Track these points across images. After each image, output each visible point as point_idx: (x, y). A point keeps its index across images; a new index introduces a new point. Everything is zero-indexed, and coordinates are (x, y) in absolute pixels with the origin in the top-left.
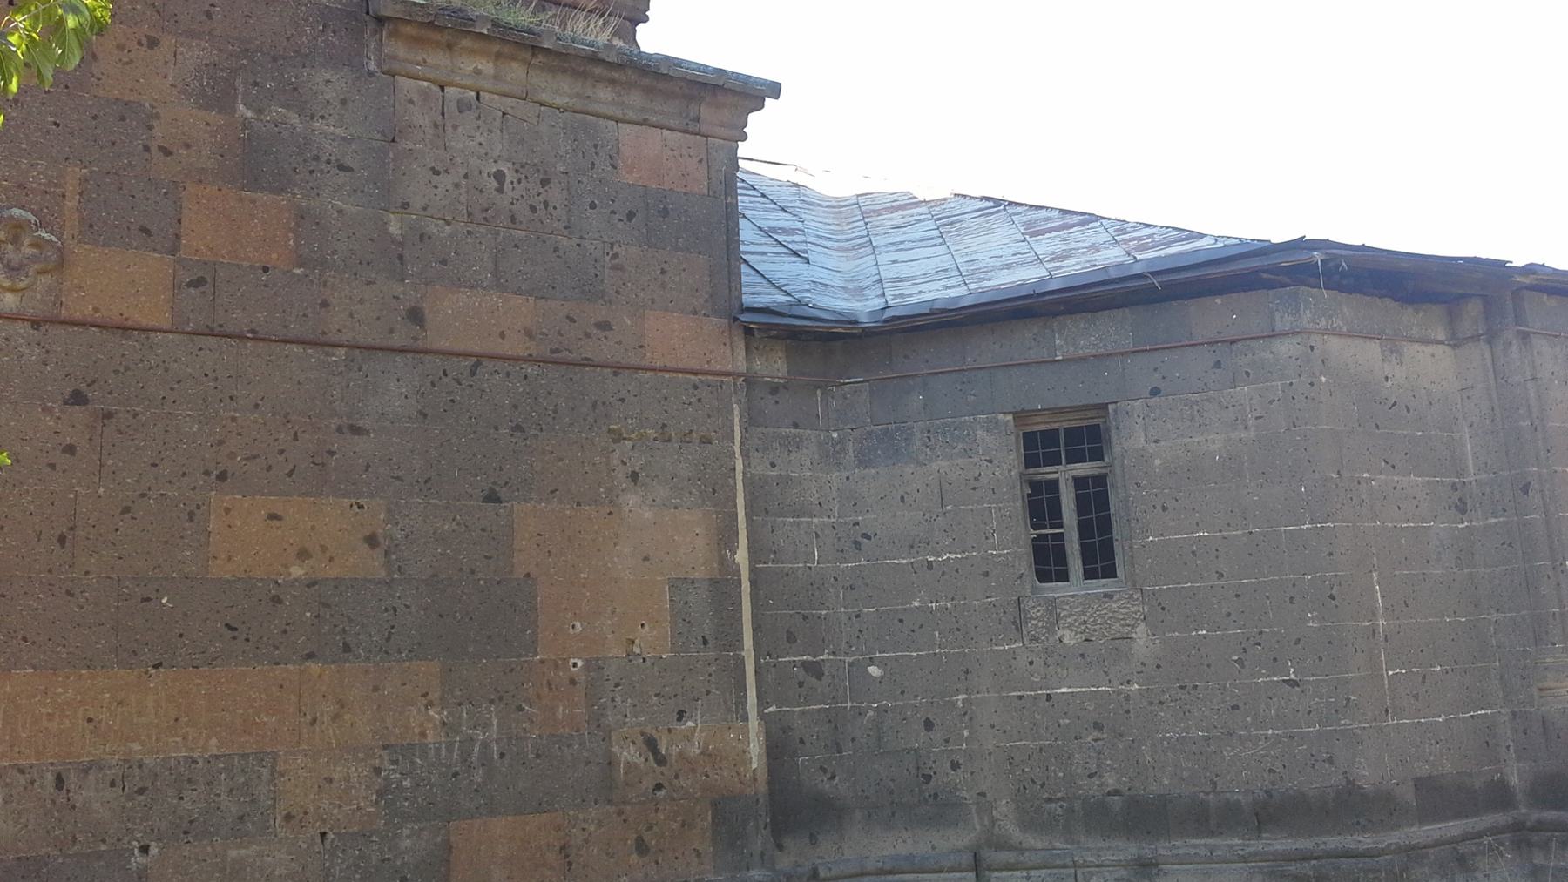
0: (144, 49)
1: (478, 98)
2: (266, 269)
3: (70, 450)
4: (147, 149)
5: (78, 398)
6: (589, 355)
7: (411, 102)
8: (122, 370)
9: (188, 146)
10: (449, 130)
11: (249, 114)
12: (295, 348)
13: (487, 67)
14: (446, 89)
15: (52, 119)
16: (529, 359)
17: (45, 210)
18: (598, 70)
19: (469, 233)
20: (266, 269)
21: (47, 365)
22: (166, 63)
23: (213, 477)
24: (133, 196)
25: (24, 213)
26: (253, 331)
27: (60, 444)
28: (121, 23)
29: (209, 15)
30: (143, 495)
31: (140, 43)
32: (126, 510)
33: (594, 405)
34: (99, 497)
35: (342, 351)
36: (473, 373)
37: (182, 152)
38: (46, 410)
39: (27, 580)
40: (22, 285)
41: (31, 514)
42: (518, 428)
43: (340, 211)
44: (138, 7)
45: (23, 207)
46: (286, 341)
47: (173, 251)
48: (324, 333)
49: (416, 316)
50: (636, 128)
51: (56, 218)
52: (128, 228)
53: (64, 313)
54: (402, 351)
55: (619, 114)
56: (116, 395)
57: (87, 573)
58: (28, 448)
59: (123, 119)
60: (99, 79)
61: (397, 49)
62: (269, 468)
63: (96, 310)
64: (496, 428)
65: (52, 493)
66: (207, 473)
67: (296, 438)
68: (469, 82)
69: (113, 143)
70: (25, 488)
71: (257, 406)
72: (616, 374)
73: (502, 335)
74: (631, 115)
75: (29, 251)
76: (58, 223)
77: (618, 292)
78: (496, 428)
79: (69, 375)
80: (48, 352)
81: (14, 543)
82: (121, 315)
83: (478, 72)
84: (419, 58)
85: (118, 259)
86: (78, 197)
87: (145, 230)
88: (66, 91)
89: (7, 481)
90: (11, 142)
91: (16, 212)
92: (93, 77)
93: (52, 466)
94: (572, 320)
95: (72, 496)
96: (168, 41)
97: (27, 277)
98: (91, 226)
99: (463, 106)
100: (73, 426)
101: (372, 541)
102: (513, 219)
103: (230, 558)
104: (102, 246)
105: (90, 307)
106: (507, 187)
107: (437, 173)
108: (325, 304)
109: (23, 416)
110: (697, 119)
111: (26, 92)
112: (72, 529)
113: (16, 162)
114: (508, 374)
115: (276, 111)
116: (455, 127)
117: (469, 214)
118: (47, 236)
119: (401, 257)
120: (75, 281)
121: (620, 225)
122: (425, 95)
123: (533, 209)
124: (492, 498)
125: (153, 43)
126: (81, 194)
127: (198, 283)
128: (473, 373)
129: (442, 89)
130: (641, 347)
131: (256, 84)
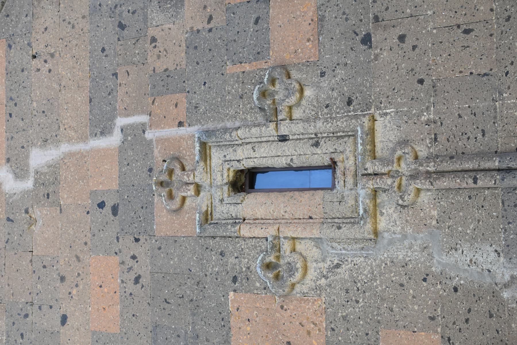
0: (157, 44)
3: (402, 38)
4: (210, 30)
5: (367, 40)
8: (345, 16)
9: (205, 7)
15: (203, 86)
17: (253, 81)
21: (347, 63)
22: (163, 30)
24: (238, 32)
25: (255, 92)
27: (399, 45)
28: (146, 59)
31: (155, 47)
34: (434, 13)
38: (377, 57)
39: (499, 50)
40: (297, 86)
41: (450, 55)
44: (137, 52)
51: (257, 74)
52: (257, 31)
56: (362, 17)
57: (492, 10)
58: (403, 65)
59: (196, 48)
60: (177, 65)
63: (309, 40)
65: (434, 44)
69: (210, 50)
70: (431, 62)
75: (277, 86)
76: (259, 73)
79: (352, 48)
80: (338, 64)
81: (472, 63)
82: (310, 24)
85: (276, 33)
86: (243, 64)
88: (186, 82)
89: (427, 74)
90: (218, 107)
91: (255, 97)
92: (176, 69)
93: (414, 47)
95: (435, 31)
96: (151, 32)
97: (291, 84)
98: (258, 53)
100: (386, 39)
104: (269, 44)
105: (308, 44)
109: (382, 72)
111: (190, 103)
113: (229, 102)
118: (267, 77)
120: (292, 56)
125: (154, 40)
126: (241, 63)
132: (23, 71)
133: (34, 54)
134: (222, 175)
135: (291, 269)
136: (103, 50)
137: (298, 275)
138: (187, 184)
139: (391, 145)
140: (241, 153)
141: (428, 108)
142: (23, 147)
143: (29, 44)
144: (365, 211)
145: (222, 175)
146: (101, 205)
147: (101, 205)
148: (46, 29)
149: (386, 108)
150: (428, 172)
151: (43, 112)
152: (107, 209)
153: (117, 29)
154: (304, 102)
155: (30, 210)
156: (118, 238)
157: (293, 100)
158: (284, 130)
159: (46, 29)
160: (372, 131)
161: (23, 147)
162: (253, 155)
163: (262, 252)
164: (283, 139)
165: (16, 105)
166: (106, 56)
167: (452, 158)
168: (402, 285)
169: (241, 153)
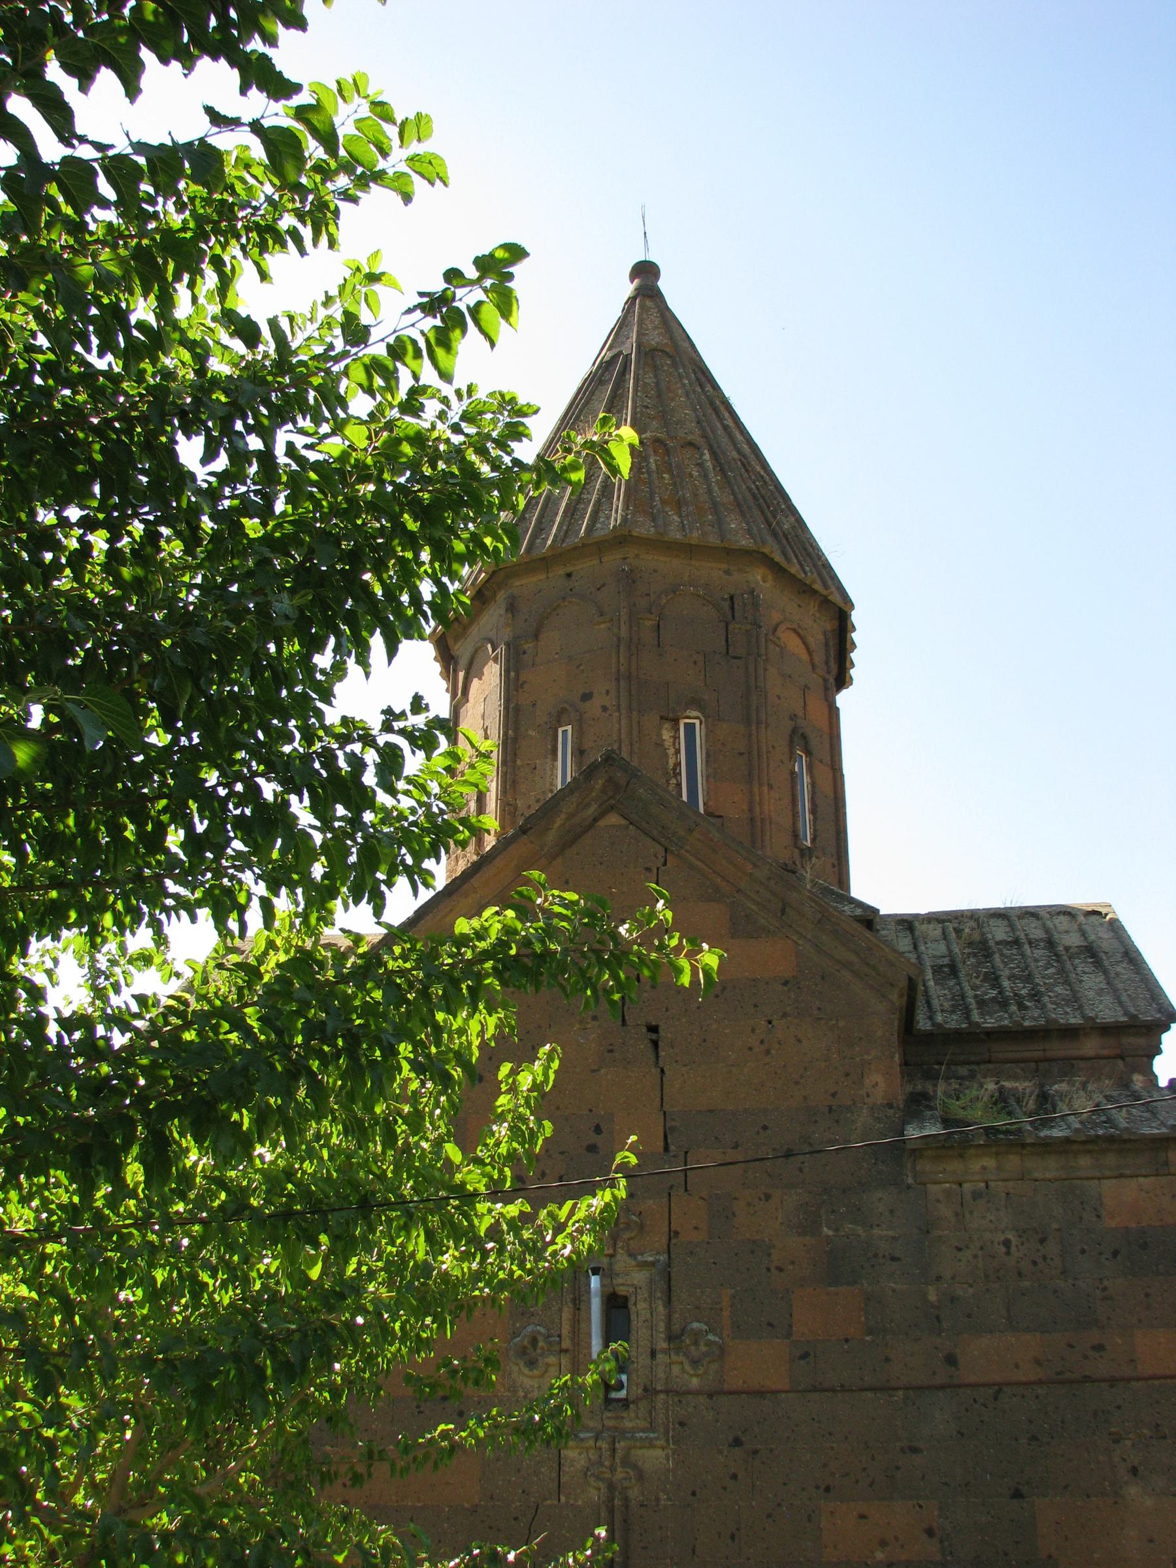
1: (987, 1187)
2: (847, 1340)
3: (734, 1477)
4: (769, 1270)
5: (737, 1442)
6: (1087, 1373)
7: (938, 1201)
9: (793, 1263)
10: (967, 1215)
11: (831, 1233)
12: (870, 1394)
13: (990, 1162)
14: (966, 1186)
16: (1040, 1382)
18: (1075, 1147)
19: (988, 1290)
20: (847, 1340)
23: (821, 1490)
26: (842, 1386)
29: (801, 1170)
30: (779, 1505)
31: (760, 1199)
32: (769, 1516)
33: (1095, 1414)
35: (901, 1393)
36: (996, 1398)
37: (791, 1267)
38: (720, 1452)
40: (700, 1372)
42: (1034, 1438)
43: (894, 1291)
45: (699, 1321)
46: (862, 1390)
47: (789, 1335)
48: (888, 1381)
49: (951, 1360)
50: (1114, 1181)
53: (726, 1387)
54: (942, 1387)
55: (1098, 1174)
59: (753, 1252)
61: (924, 1166)
62: (857, 1482)
63: (744, 1382)
64: (1016, 1439)
66: (817, 1487)
67: (873, 1459)
68: (977, 1178)
71: (846, 1438)
72: (1112, 1386)
73: (1017, 1366)
74: (1107, 1173)
75: (703, 1348)
77: (1109, 1318)
78: (1016, 1439)
83: (984, 1168)
84: (940, 1169)
87: (770, 1325)
93: (725, 1488)
94: (1071, 1346)
99: (976, 1195)
101: (930, 1532)
102: (1020, 1274)
103: (835, 1546)
106: (1013, 1249)
107: (959, 1249)
108: (887, 1360)
110: (1166, 1163)
112: (738, 1529)
114: (1023, 1396)
115: (848, 1227)
116: (971, 1213)
117: (986, 1276)
119: (938, 1318)
121: (1107, 1263)
122: (947, 1193)
123: (1035, 1263)
124: (1017, 1495)
125: (768, 1197)
127: (805, 1356)
128: (996, 1398)
129: (960, 1185)
130: (1132, 1361)
131: (833, 1211)
132: (756, 1006)
133: (775, 1022)
134: (623, 1285)
135: (532, 1364)
136: (765, 1128)
137: (526, 1371)
138: (615, 1244)
139: (640, 1464)
140: (642, 1306)
141: (669, 1499)
142: (667, 1010)
143: (785, 1015)
144: (582, 1440)
145: (623, 1285)
146: (598, 1130)
147: (598, 1130)
148: (799, 1041)
149: (674, 1460)
150: (613, 1499)
151: (705, 1041)
152: (594, 1138)
153: (786, 1147)
154: (686, 1376)
155: (596, 1023)
156: (562, 1153)
157: (687, 1367)
158: (660, 1357)
159: (799, 1041)
160: (652, 1446)
161: (667, 1010)
162: (641, 1319)
163: (548, 1330)
164: (653, 1354)
165: (717, 996)
166: (758, 1133)
167: (625, 1521)
168: (519, 1471)
169: (642, 1306)
